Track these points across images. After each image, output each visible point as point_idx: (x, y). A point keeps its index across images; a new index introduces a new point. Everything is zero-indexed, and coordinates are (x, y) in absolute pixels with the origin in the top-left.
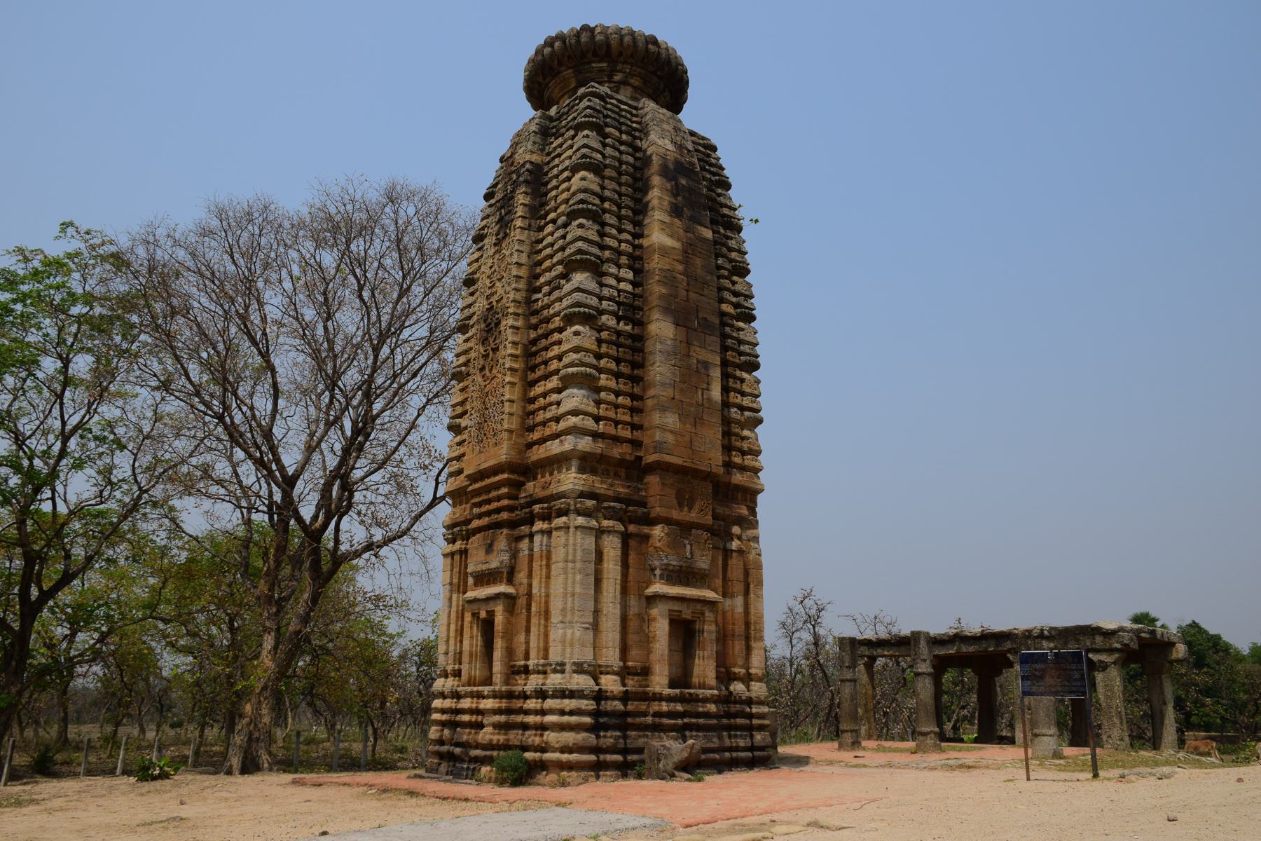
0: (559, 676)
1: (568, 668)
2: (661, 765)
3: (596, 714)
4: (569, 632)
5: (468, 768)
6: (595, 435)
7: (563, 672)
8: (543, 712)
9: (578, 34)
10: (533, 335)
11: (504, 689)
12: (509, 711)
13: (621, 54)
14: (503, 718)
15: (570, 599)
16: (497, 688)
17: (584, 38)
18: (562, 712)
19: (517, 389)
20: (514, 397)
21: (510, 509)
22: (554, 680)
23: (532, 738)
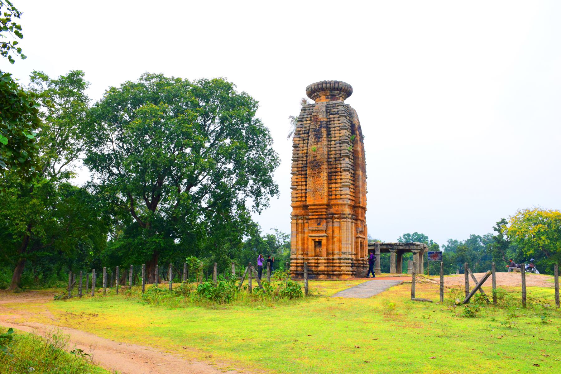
8: (340, 263)
10: (330, 171)
12: (328, 263)
14: (327, 265)
22: (343, 256)
23: (338, 269)
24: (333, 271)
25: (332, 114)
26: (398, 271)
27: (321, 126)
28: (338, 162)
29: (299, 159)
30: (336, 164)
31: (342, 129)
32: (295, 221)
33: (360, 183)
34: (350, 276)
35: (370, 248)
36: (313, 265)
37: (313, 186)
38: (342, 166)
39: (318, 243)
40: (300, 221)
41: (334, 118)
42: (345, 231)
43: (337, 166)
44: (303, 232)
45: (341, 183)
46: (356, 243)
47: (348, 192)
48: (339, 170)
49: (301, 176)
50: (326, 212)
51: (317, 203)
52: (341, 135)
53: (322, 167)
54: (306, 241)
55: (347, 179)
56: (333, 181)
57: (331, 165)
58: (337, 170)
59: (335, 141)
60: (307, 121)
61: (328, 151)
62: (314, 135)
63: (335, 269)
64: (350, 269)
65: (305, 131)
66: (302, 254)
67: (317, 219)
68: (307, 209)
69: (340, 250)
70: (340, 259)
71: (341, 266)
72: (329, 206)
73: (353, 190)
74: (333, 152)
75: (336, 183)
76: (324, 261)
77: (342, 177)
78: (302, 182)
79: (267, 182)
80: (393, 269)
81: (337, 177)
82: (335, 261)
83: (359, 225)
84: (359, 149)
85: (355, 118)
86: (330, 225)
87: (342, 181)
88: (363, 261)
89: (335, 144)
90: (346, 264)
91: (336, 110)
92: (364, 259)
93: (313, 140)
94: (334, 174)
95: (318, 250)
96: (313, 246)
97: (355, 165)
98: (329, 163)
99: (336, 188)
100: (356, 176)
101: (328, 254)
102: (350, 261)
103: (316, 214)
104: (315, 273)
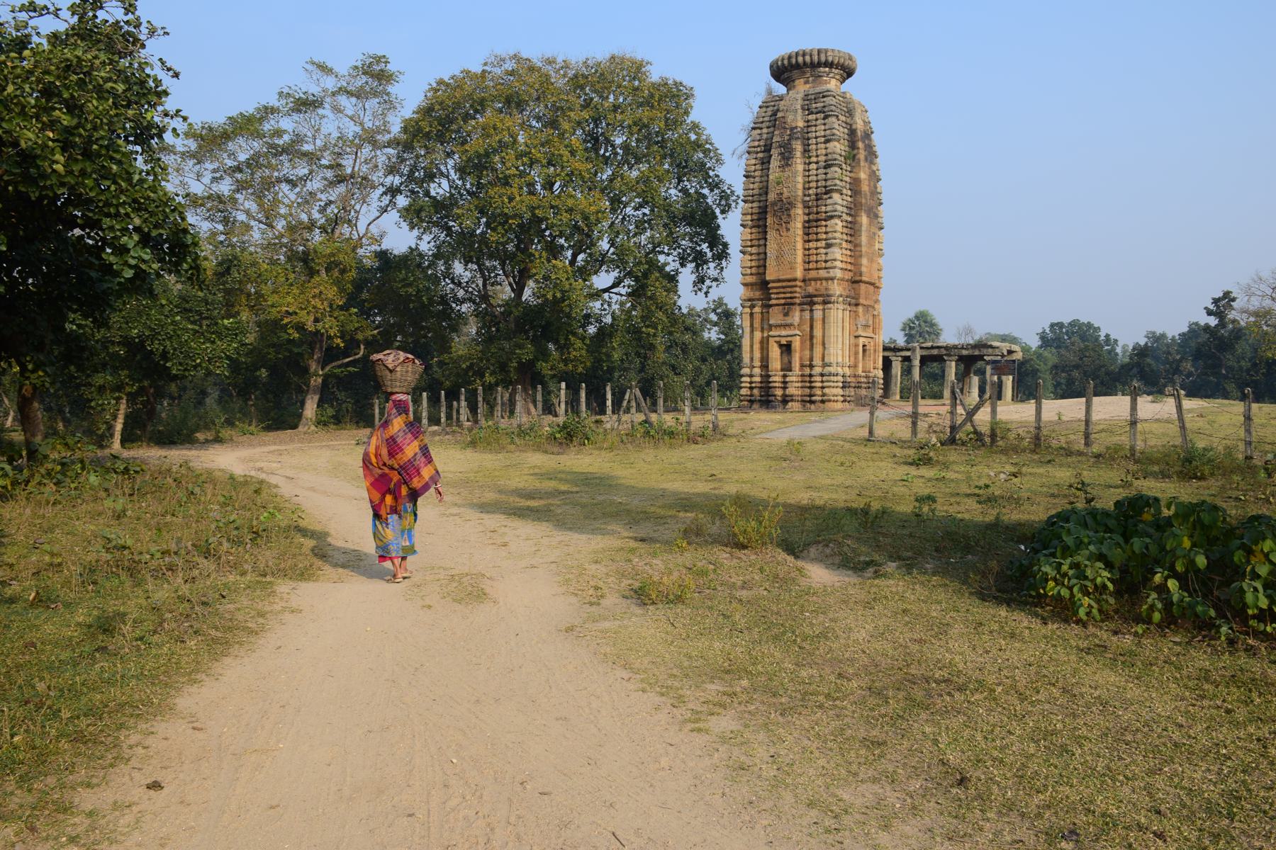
27: (791, 137)
28: (820, 202)
58: (819, 216)
59: (817, 163)
73: (849, 253)
75: (817, 240)
79: (714, 239)
88: (867, 377)
101: (802, 366)
102: (840, 379)
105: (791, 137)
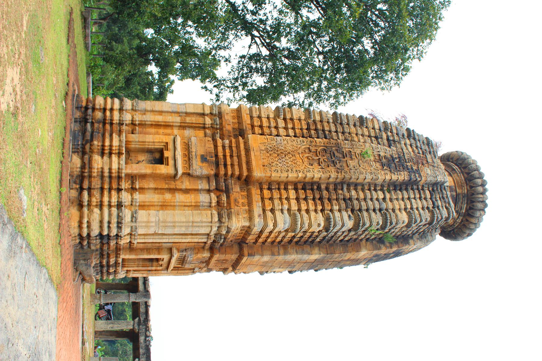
0: (130, 220)
1: (133, 224)
2: (82, 262)
3: (108, 235)
4: (153, 224)
5: (78, 145)
6: (261, 232)
7: (132, 221)
8: (110, 206)
9: (483, 202)
10: (323, 187)
11: (123, 175)
12: (110, 177)
13: (467, 220)
14: (106, 174)
15: (172, 224)
16: (124, 171)
17: (480, 205)
18: (109, 222)
19: (294, 180)
20: (289, 178)
21: (226, 174)
22: (127, 214)
23: (94, 200)
24: (89, 189)
25: (431, 195)
26: (97, 333)
27: (410, 171)
28: (343, 205)
29: (339, 126)
30: (337, 199)
31: (409, 214)
32: (207, 111)
33: (293, 257)
34: (76, 231)
35: (141, 283)
36: (107, 143)
37: (289, 148)
38: (337, 214)
39: (159, 158)
40: (208, 121)
41: (425, 199)
42: (189, 218)
43: (334, 202)
44: (183, 126)
45: (299, 210)
46: (159, 249)
47: (281, 226)
48: (328, 207)
49: (305, 127)
50: (232, 175)
51: (253, 157)
52: (397, 211)
53: (332, 169)
54: (161, 131)
55: (310, 225)
56: (301, 192)
57: (335, 189)
58: (326, 201)
59: (384, 199)
60: (411, 145)
61: (363, 185)
62: (392, 156)
63: (96, 194)
64: (95, 232)
65: (394, 141)
66: (133, 124)
67: (216, 156)
68: (236, 137)
69: (143, 206)
70: (120, 206)
71: (101, 209)
72: (247, 182)
73: (279, 239)
74: (362, 195)
75: (297, 199)
76: (115, 166)
77: (313, 214)
78: (293, 128)
80: (103, 325)
81: (311, 202)
82: (114, 193)
83: (199, 256)
84: (364, 253)
85: (419, 244)
86: (203, 185)
87: (303, 213)
88: (116, 264)
89: (377, 199)
90: (106, 219)
91: (440, 204)
92: (120, 269)
93: (382, 154)
94: (317, 196)
95: (142, 157)
96: (151, 147)
97: (331, 245)
98: (338, 185)
99: (288, 199)
100: (307, 248)
101: (132, 178)
102: (114, 232)
103: (228, 154)
104: (88, 147)
105: (410, 171)
